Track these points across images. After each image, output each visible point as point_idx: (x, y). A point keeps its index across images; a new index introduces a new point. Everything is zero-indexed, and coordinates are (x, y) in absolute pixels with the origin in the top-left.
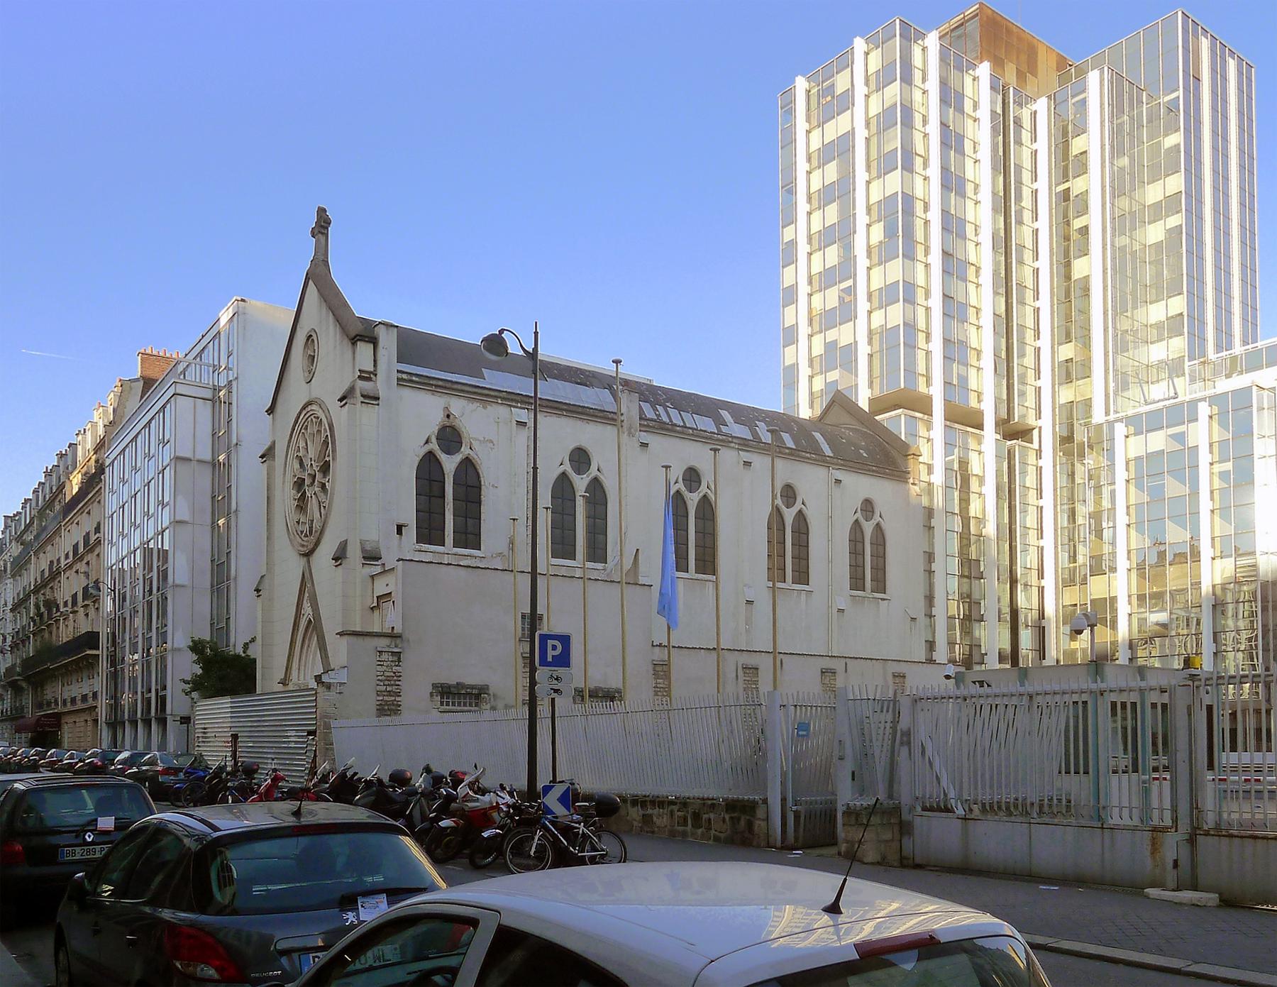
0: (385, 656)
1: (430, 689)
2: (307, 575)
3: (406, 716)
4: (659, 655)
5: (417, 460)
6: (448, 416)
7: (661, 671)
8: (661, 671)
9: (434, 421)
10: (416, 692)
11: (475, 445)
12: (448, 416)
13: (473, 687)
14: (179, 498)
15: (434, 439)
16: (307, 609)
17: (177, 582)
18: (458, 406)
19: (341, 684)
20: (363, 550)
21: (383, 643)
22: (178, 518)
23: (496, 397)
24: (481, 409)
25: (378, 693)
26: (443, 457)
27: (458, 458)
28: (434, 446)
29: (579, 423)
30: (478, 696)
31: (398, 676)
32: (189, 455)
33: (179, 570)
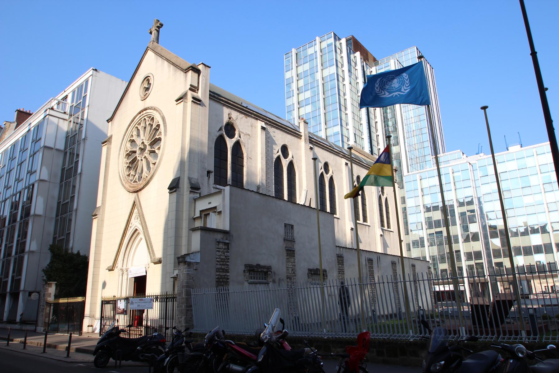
0: (221, 245)
1: (243, 268)
2: (137, 203)
3: (232, 288)
4: (338, 251)
5: (215, 138)
6: (230, 118)
7: (340, 259)
8: (340, 259)
10: (237, 270)
13: (264, 267)
14: (44, 168)
16: (135, 223)
17: (37, 213)
18: (235, 115)
19: (197, 263)
20: (190, 183)
21: (219, 237)
22: (41, 178)
23: (252, 113)
25: (218, 270)
26: (227, 139)
27: (234, 140)
30: (266, 273)
31: (227, 258)
32: (52, 145)
33: (38, 206)
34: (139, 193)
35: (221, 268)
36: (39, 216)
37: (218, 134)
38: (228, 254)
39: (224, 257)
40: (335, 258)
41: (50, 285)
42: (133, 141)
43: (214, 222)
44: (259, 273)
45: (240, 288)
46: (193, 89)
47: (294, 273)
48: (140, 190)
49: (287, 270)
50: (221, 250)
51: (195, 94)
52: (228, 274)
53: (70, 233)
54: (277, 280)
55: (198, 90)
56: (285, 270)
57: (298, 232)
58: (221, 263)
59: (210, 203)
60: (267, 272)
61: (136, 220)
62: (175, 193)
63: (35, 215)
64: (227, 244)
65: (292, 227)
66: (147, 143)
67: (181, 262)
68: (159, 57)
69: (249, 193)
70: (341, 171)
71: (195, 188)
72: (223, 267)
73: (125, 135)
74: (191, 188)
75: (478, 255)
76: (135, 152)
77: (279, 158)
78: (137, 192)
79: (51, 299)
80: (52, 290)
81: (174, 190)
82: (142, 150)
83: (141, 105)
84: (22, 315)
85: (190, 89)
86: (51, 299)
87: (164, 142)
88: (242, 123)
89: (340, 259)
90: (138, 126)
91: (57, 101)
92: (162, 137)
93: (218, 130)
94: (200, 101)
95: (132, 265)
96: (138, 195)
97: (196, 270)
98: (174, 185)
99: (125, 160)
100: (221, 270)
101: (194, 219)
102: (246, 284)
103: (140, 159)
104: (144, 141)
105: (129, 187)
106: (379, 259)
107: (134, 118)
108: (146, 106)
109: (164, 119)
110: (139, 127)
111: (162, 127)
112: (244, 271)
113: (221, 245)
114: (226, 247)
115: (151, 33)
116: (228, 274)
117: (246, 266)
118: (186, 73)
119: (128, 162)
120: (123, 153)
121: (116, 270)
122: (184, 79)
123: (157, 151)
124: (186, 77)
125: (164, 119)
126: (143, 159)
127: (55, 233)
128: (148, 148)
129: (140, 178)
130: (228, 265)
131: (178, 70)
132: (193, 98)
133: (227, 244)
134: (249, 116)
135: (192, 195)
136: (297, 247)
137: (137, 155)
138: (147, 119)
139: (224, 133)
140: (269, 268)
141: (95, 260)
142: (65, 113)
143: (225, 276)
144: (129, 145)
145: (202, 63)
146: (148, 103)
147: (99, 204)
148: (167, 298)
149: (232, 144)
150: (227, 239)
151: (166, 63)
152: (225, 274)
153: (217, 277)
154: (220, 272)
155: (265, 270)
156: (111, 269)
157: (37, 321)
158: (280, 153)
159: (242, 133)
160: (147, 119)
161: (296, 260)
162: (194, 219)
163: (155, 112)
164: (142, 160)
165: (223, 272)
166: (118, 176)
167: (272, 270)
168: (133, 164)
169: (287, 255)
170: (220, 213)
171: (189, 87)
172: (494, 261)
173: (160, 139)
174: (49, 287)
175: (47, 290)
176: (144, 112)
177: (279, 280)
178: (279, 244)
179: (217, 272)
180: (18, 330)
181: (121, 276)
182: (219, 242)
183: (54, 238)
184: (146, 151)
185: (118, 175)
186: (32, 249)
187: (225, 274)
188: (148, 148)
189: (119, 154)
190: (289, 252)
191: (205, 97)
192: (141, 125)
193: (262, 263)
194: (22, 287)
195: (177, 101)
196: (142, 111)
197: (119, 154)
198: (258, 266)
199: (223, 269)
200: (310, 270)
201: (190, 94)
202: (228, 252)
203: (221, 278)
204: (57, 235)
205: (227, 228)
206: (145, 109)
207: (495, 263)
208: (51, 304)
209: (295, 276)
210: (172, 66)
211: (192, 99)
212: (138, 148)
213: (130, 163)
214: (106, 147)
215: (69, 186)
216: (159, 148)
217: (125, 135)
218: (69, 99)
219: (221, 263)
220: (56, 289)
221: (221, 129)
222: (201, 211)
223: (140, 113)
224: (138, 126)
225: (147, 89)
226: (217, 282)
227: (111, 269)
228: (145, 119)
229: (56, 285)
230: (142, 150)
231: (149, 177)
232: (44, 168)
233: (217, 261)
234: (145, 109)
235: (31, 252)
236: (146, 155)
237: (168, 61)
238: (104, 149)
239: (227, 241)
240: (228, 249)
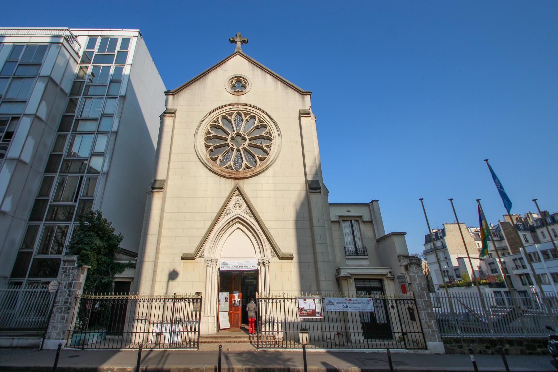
48: (244, 178)
59: (349, 211)
61: (237, 208)
68: (255, 67)
73: (206, 117)
78: (238, 179)
83: (233, 99)
103: (235, 148)
104: (241, 132)
105: (220, 171)
107: (224, 106)
115: (234, 42)
128: (248, 140)
164: (238, 150)
176: (242, 107)
196: (238, 104)
212: (230, 136)
213: (214, 147)
217: (206, 117)
222: (340, 217)
223: (233, 105)
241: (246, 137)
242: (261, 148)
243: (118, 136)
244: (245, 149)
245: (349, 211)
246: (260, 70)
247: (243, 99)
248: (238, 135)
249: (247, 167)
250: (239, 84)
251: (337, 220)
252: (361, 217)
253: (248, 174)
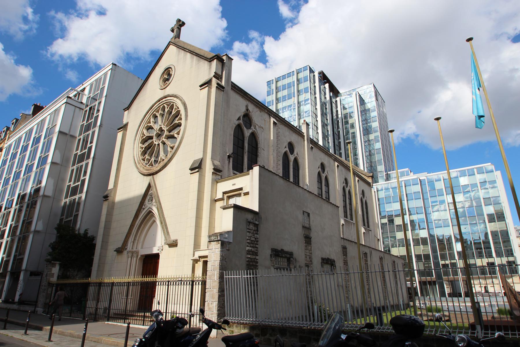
3: (261, 272)
5: (235, 126)
9: (243, 110)
10: (264, 255)
11: (257, 127)
12: (247, 110)
13: (287, 253)
14: (57, 151)
15: (241, 118)
17: (46, 194)
18: (251, 107)
21: (250, 217)
24: (259, 112)
27: (250, 131)
28: (241, 121)
29: (291, 132)
31: (257, 241)
34: (155, 176)
35: (251, 251)
36: (48, 197)
37: (237, 123)
38: (258, 236)
39: (253, 239)
40: (340, 249)
41: (54, 265)
42: (149, 128)
43: (240, 201)
44: (282, 257)
45: (267, 274)
46: (218, 76)
47: (311, 261)
48: (157, 173)
49: (306, 257)
50: (252, 231)
51: (219, 82)
52: (257, 257)
53: (78, 214)
54: (297, 267)
55: (221, 78)
56: (304, 257)
57: (315, 222)
58: (252, 245)
59: (234, 184)
60: (290, 258)
62: (198, 173)
63: (44, 196)
64: (256, 226)
65: (309, 215)
66: (165, 128)
67: (214, 241)
68: (181, 50)
69: (275, 176)
70: (334, 173)
71: (217, 171)
72: (253, 249)
74: (214, 169)
75: (427, 257)
76: (151, 138)
77: (286, 153)
79: (54, 279)
80: (56, 270)
81: (197, 170)
82: (159, 136)
83: (160, 94)
84: (21, 295)
85: (214, 76)
86: (54, 279)
87: (185, 126)
88: (256, 115)
89: (344, 250)
90: (157, 114)
91: (76, 92)
92: (183, 122)
93: (237, 118)
94: (223, 88)
95: (142, 248)
96: (153, 178)
97: (228, 250)
98: (197, 165)
99: (140, 145)
100: (251, 253)
101: (216, 201)
102: (272, 268)
104: (162, 126)
106: (371, 253)
108: (166, 94)
109: (185, 105)
110: (158, 114)
111: (182, 112)
112: (271, 255)
113: (251, 226)
114: (256, 229)
116: (257, 257)
117: (273, 250)
118: (210, 62)
119: (144, 146)
120: (139, 139)
121: (125, 252)
122: (208, 67)
123: (176, 136)
124: (210, 65)
125: (185, 105)
126: (161, 144)
127: (62, 214)
129: (156, 162)
130: (257, 248)
131: (201, 60)
132: (218, 84)
133: (256, 226)
134: (262, 110)
135: (214, 177)
136: (313, 235)
137: (154, 140)
138: (166, 106)
139: (242, 123)
140: (291, 254)
141: (102, 242)
142: (82, 103)
143: (255, 258)
144: (145, 131)
145: (226, 55)
146: (169, 91)
147: (111, 186)
148: (193, 282)
149: (249, 134)
150: (256, 220)
151: (189, 55)
152: (254, 257)
153: (247, 260)
154: (250, 254)
155: (288, 256)
156: (119, 251)
157: (37, 302)
158: (287, 149)
159: (257, 125)
160: (166, 106)
161: (312, 248)
162: (216, 201)
163: (175, 99)
164: (159, 144)
165: (253, 255)
166: (133, 160)
167: (294, 256)
168: (149, 149)
169: (305, 243)
170: (247, 194)
171: (214, 74)
172: (442, 262)
173: (179, 125)
174: (53, 267)
175: (51, 270)
177: (300, 267)
178: (299, 232)
179: (247, 254)
180: (15, 310)
181: (130, 259)
182: (250, 222)
183: (61, 220)
184: (164, 136)
185: (133, 158)
186: (37, 229)
187: (254, 257)
188: (166, 133)
189: (135, 139)
190: (307, 240)
191: (228, 85)
192: (160, 112)
193: (286, 249)
194: (24, 266)
195: (201, 86)
196: (162, 99)
197: (135, 139)
198: (282, 250)
199: (253, 252)
200: (323, 259)
201: (214, 81)
202: (257, 234)
203: (251, 261)
204: (64, 217)
205: (256, 208)
206: (165, 97)
207: (442, 265)
208: (53, 284)
209: (312, 264)
210: (195, 57)
211: (216, 85)
214: (121, 132)
215: (81, 171)
216: (178, 133)
218: (87, 92)
219: (252, 245)
220: (60, 269)
221: (239, 119)
222: (224, 193)
224: (157, 114)
225: (168, 80)
226: (247, 265)
227: (119, 251)
228: (164, 107)
229: (60, 264)
230: (159, 136)
231: (166, 160)
232: (57, 151)
233: (248, 243)
234: (165, 97)
235: (36, 232)
236: (164, 139)
237: (192, 52)
238: (120, 135)
239: (257, 223)
240: (257, 231)
241: (165, 130)
242: (173, 137)
243: (96, 160)
244: (164, 143)
245: (234, 184)
246: (183, 51)
247: (169, 91)
248: (161, 130)
249: (163, 160)
250: (167, 76)
251: (221, 197)
252: (241, 189)
253: (159, 168)
